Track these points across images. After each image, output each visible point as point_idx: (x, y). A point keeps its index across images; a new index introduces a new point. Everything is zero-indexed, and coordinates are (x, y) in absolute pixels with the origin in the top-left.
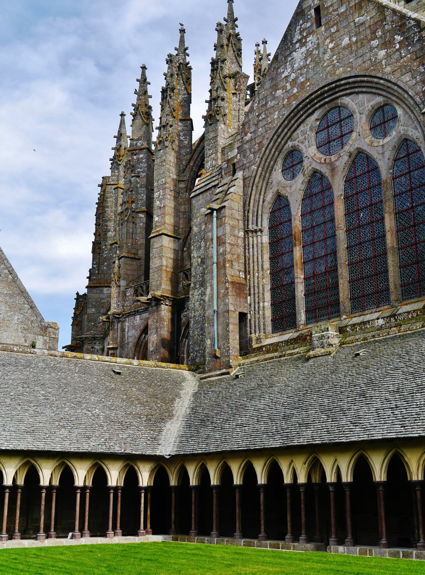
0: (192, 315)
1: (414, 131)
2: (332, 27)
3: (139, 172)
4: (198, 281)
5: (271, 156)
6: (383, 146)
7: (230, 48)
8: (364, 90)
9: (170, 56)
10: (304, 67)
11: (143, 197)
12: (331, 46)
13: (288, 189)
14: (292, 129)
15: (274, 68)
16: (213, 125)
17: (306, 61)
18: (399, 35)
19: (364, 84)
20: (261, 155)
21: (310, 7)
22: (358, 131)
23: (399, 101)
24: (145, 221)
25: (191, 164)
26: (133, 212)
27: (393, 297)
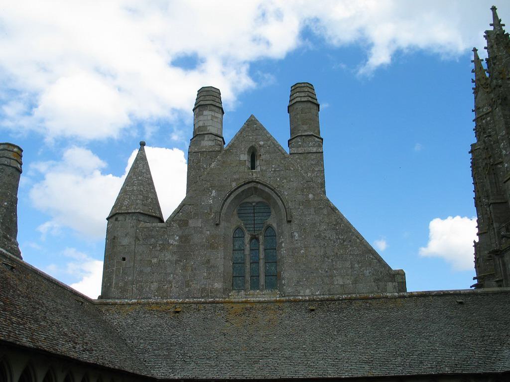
3: (489, 132)
9: (487, 32)
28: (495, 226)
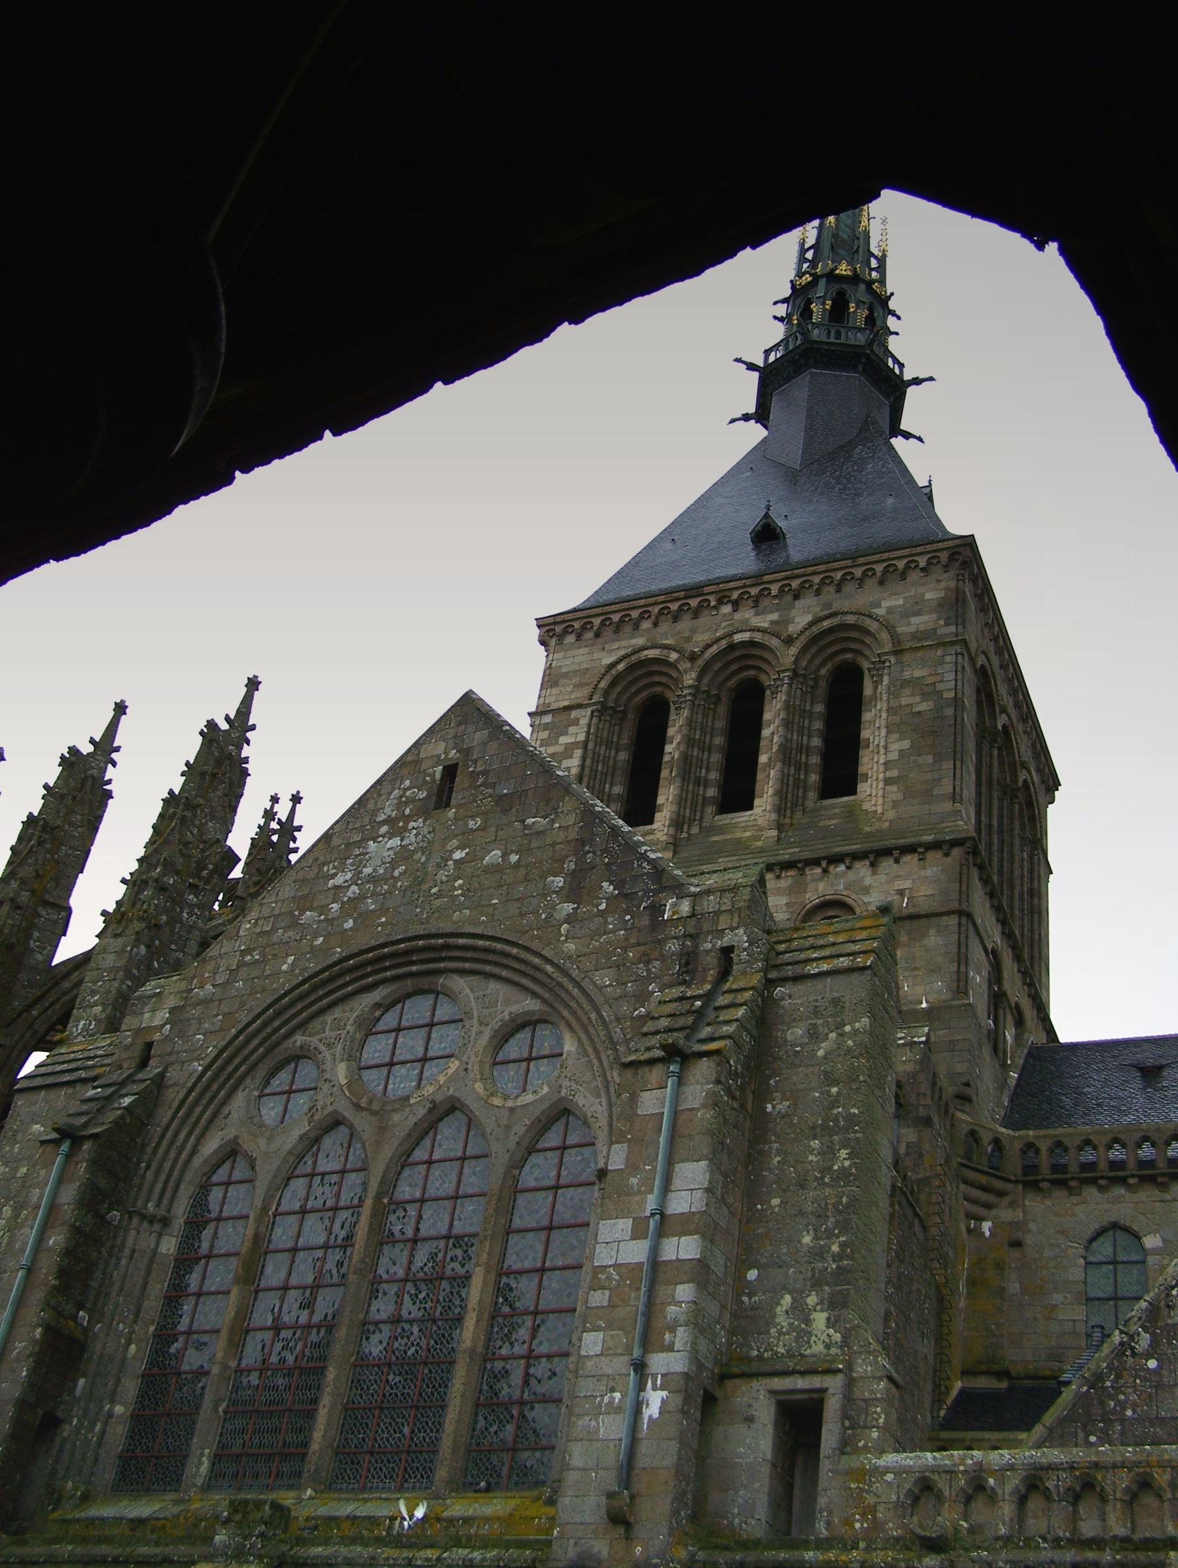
1: (591, 1099)
2: (473, 817)
5: (246, 1052)
6: (512, 1109)
8: (504, 973)
9: (73, 750)
10: (383, 879)
12: (458, 855)
13: (262, 1142)
15: (317, 859)
16: (119, 940)
17: (393, 870)
20: (223, 1043)
23: (574, 1023)
25: (35, 1013)
27: (442, 1473)
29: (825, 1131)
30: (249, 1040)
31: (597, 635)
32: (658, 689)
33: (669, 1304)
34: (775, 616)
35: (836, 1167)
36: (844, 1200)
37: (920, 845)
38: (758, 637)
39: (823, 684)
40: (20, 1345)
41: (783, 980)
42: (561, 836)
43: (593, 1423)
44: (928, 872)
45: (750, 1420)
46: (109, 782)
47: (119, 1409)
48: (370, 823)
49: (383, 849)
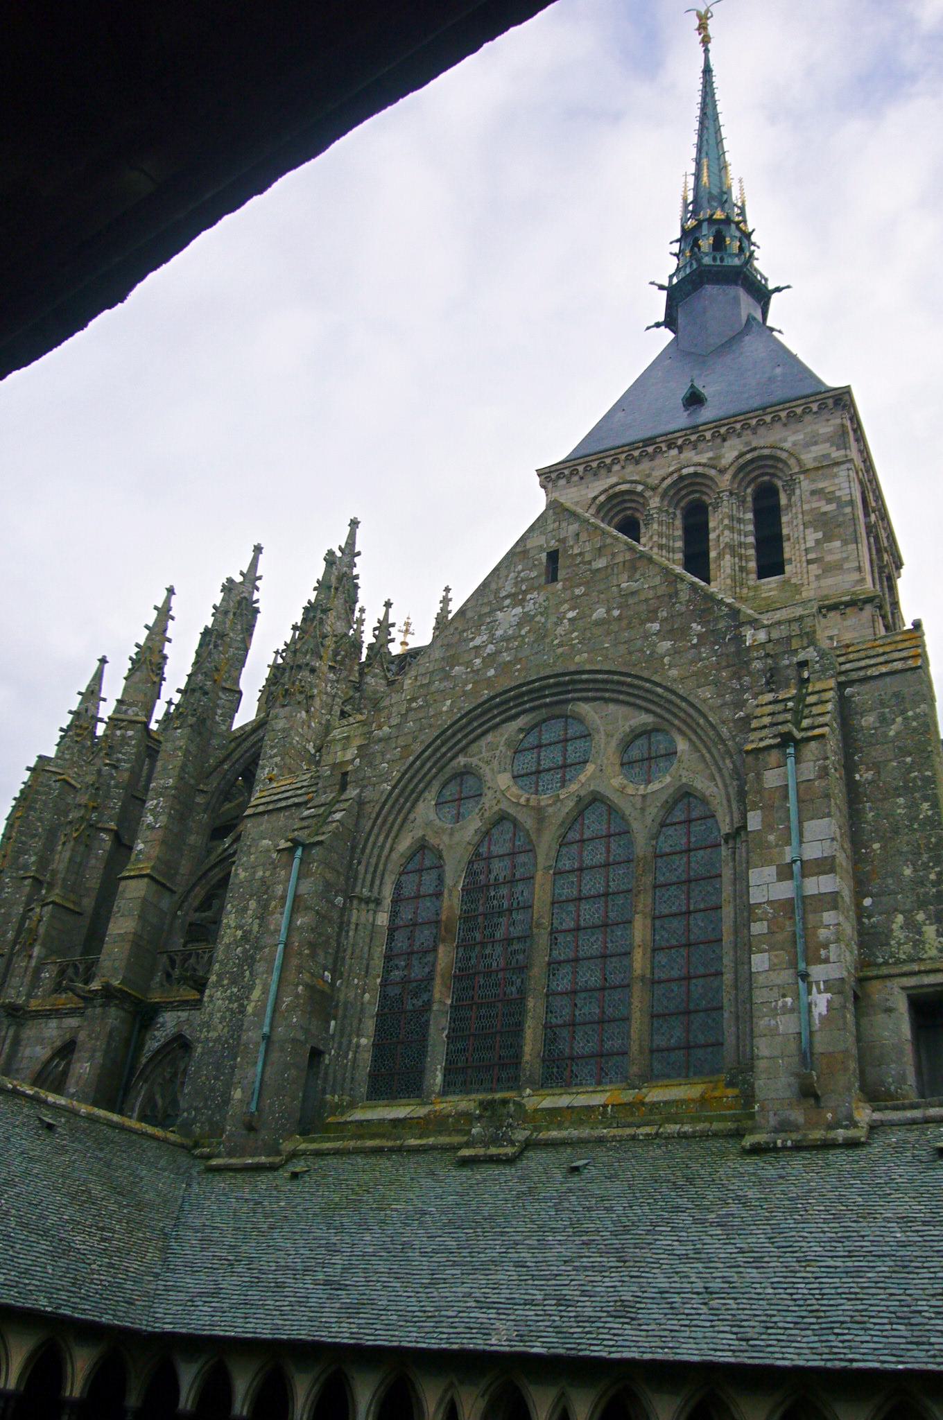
0: (202, 1036)
1: (707, 783)
2: (579, 585)
3: (118, 760)
4: (227, 973)
6: (644, 796)
7: (339, 594)
8: (621, 697)
9: (230, 580)
10: (514, 638)
11: (115, 804)
12: (571, 615)
13: (445, 838)
14: (472, 736)
15: (456, 629)
16: (286, 708)
18: (699, 624)
19: (624, 688)
20: (404, 768)
21: (541, 548)
22: (599, 762)
23: (684, 728)
24: (108, 848)
26: (91, 826)
28: (35, 954)
29: (906, 790)
30: (423, 765)
31: (582, 478)
32: (629, 512)
33: (819, 928)
34: (710, 454)
35: (921, 817)
36: (933, 840)
37: (842, 603)
38: (700, 470)
39: (749, 499)
40: (287, 1000)
41: (851, 683)
42: (651, 594)
43: (773, 1022)
44: (848, 623)
45: (889, 1010)
46: (257, 601)
47: (364, 1041)
48: (495, 598)
49: (508, 618)
